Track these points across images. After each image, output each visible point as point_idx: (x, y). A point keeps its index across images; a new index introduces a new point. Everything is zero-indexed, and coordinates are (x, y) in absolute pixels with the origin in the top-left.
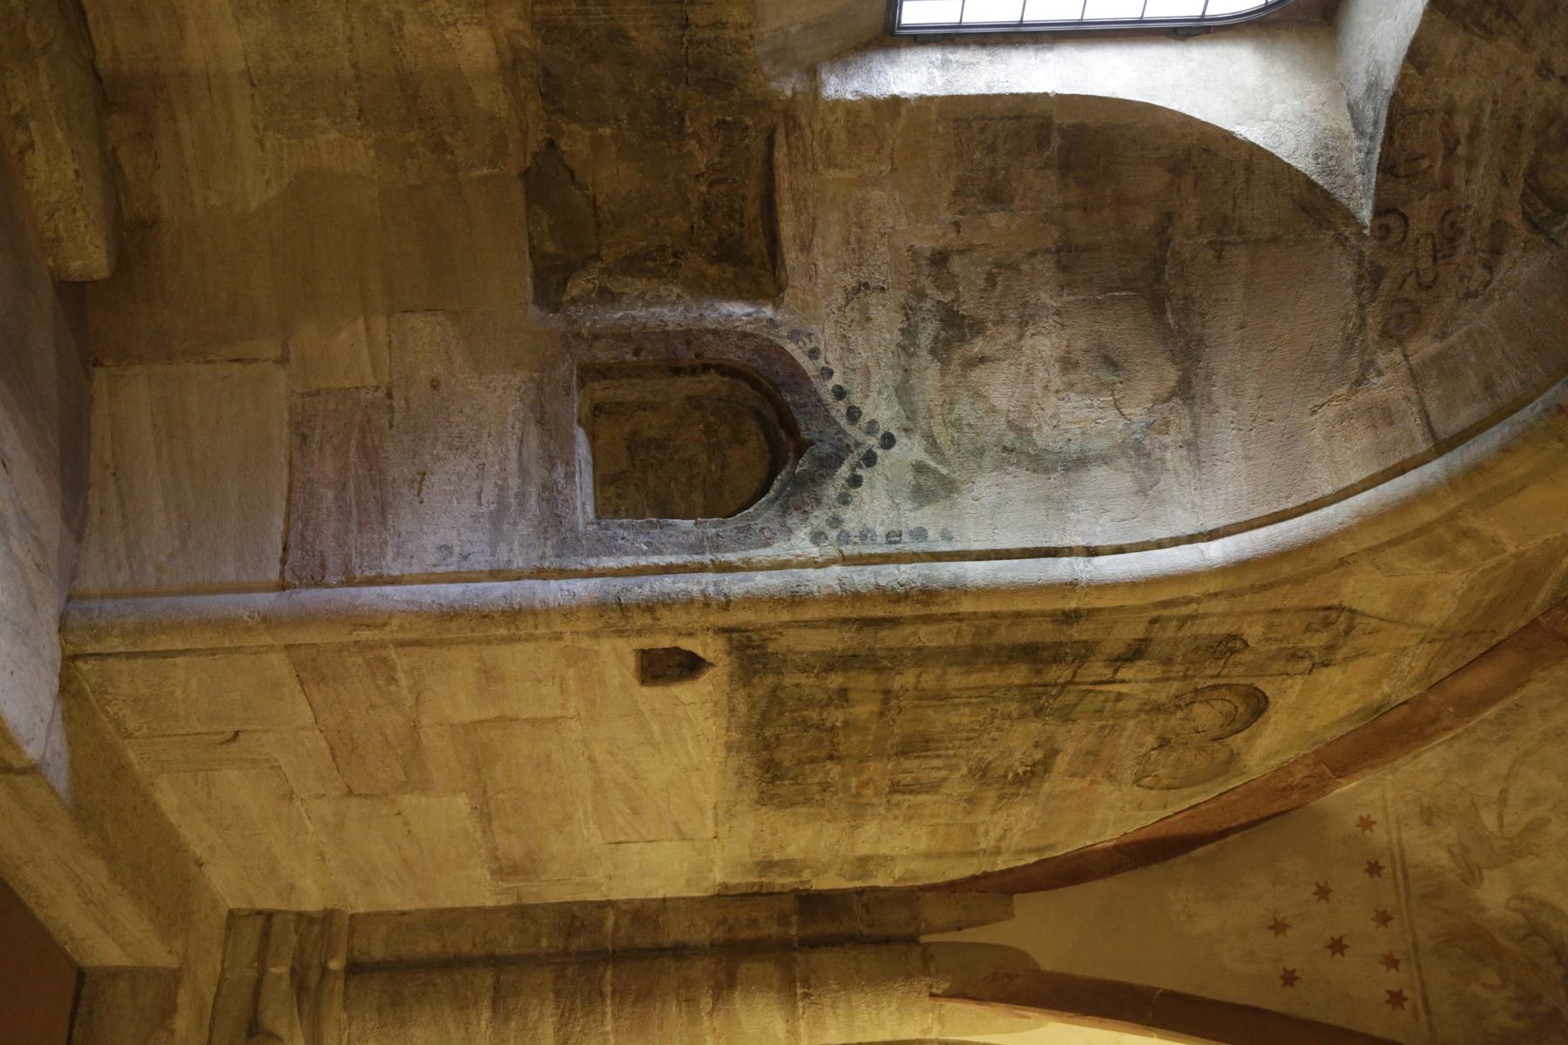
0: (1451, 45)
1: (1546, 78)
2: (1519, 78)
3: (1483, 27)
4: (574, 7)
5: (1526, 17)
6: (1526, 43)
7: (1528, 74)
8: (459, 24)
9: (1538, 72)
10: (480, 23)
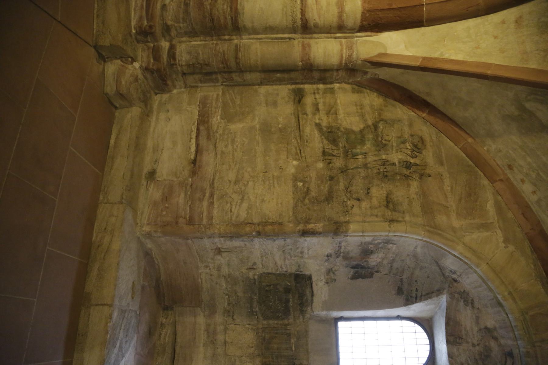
0: (455, 350)
1: (475, 347)
2: (470, 350)
3: (458, 343)
4: (271, 360)
5: (464, 337)
6: (467, 342)
7: (471, 348)
8: (247, 363)
9: (473, 346)
10: (251, 363)
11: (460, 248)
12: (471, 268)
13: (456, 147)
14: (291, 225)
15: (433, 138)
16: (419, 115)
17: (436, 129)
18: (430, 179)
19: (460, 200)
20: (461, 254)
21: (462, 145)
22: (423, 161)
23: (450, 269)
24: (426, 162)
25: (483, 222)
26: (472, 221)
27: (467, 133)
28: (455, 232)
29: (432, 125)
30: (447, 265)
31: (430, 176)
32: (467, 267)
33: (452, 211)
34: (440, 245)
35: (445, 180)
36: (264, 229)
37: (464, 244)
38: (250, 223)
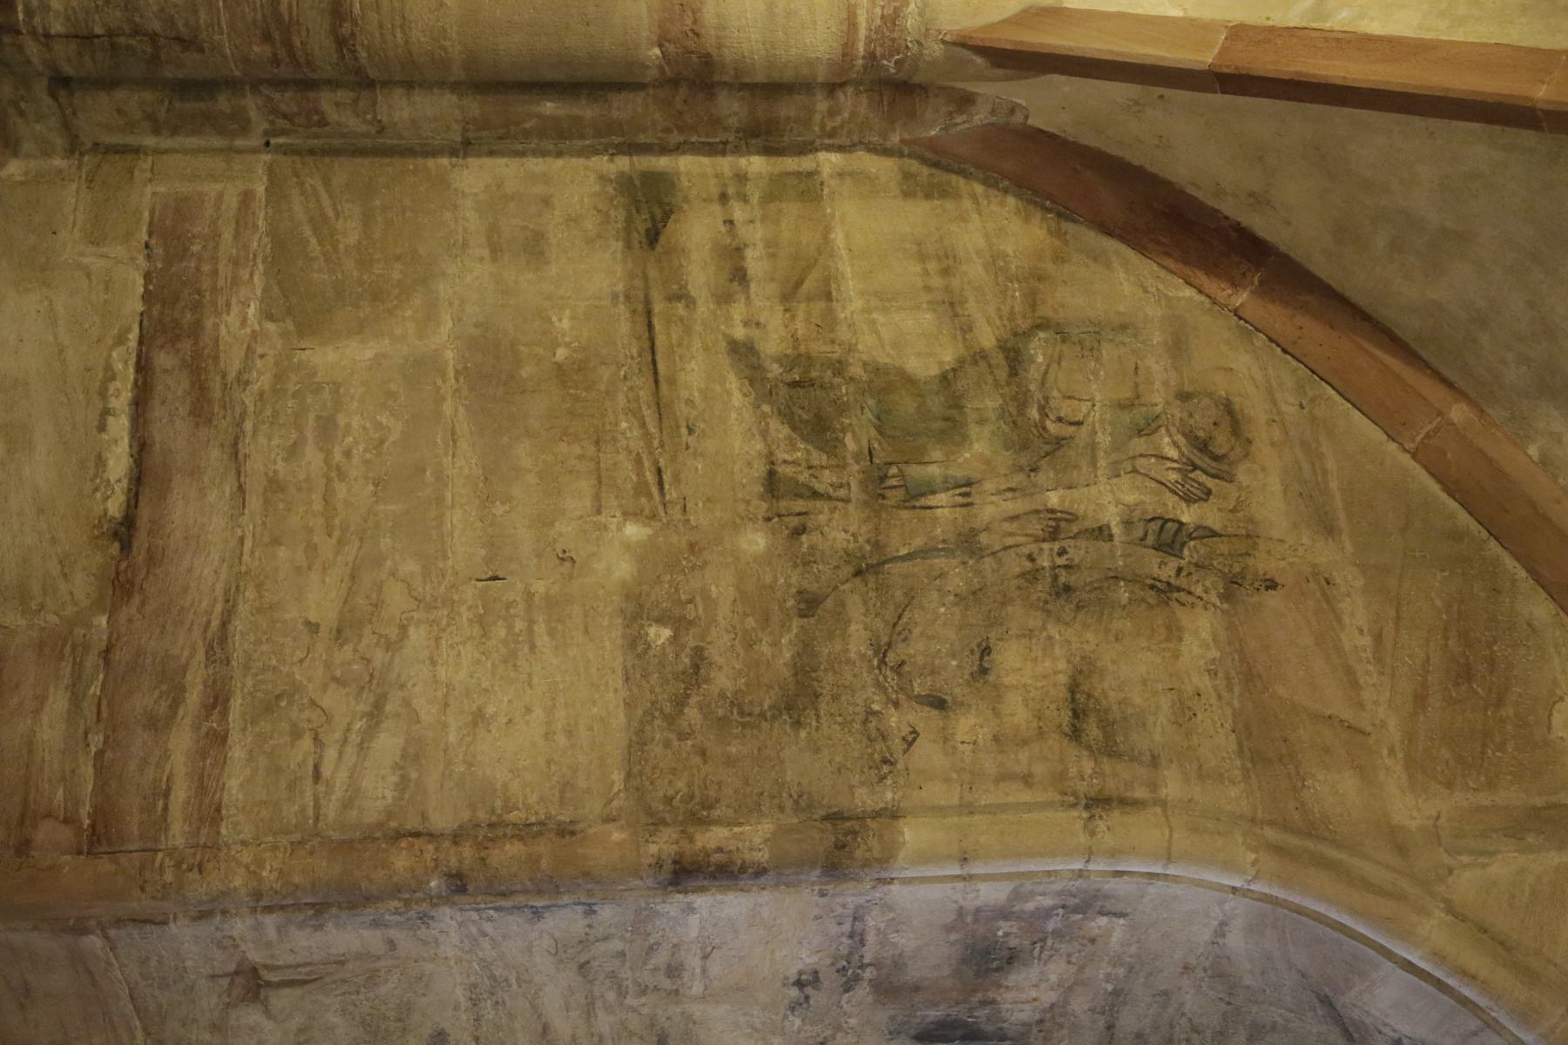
11: (1434, 927)
12: (1493, 1026)
13: (1393, 446)
14: (617, 836)
15: (1284, 408)
16: (1214, 302)
17: (1295, 363)
18: (1273, 599)
19: (1420, 700)
20: (1438, 956)
21: (1418, 439)
22: (1241, 515)
23: (1396, 1036)
24: (1251, 520)
25: (1539, 801)
26: (1484, 799)
27: (1450, 385)
28: (1402, 850)
29: (1278, 345)
30: (1373, 1011)
31: (1272, 585)
32: (1473, 1024)
33: (1385, 752)
34: (1334, 915)
35: (1345, 605)
36: (483, 859)
37: (1450, 909)
38: (417, 835)
